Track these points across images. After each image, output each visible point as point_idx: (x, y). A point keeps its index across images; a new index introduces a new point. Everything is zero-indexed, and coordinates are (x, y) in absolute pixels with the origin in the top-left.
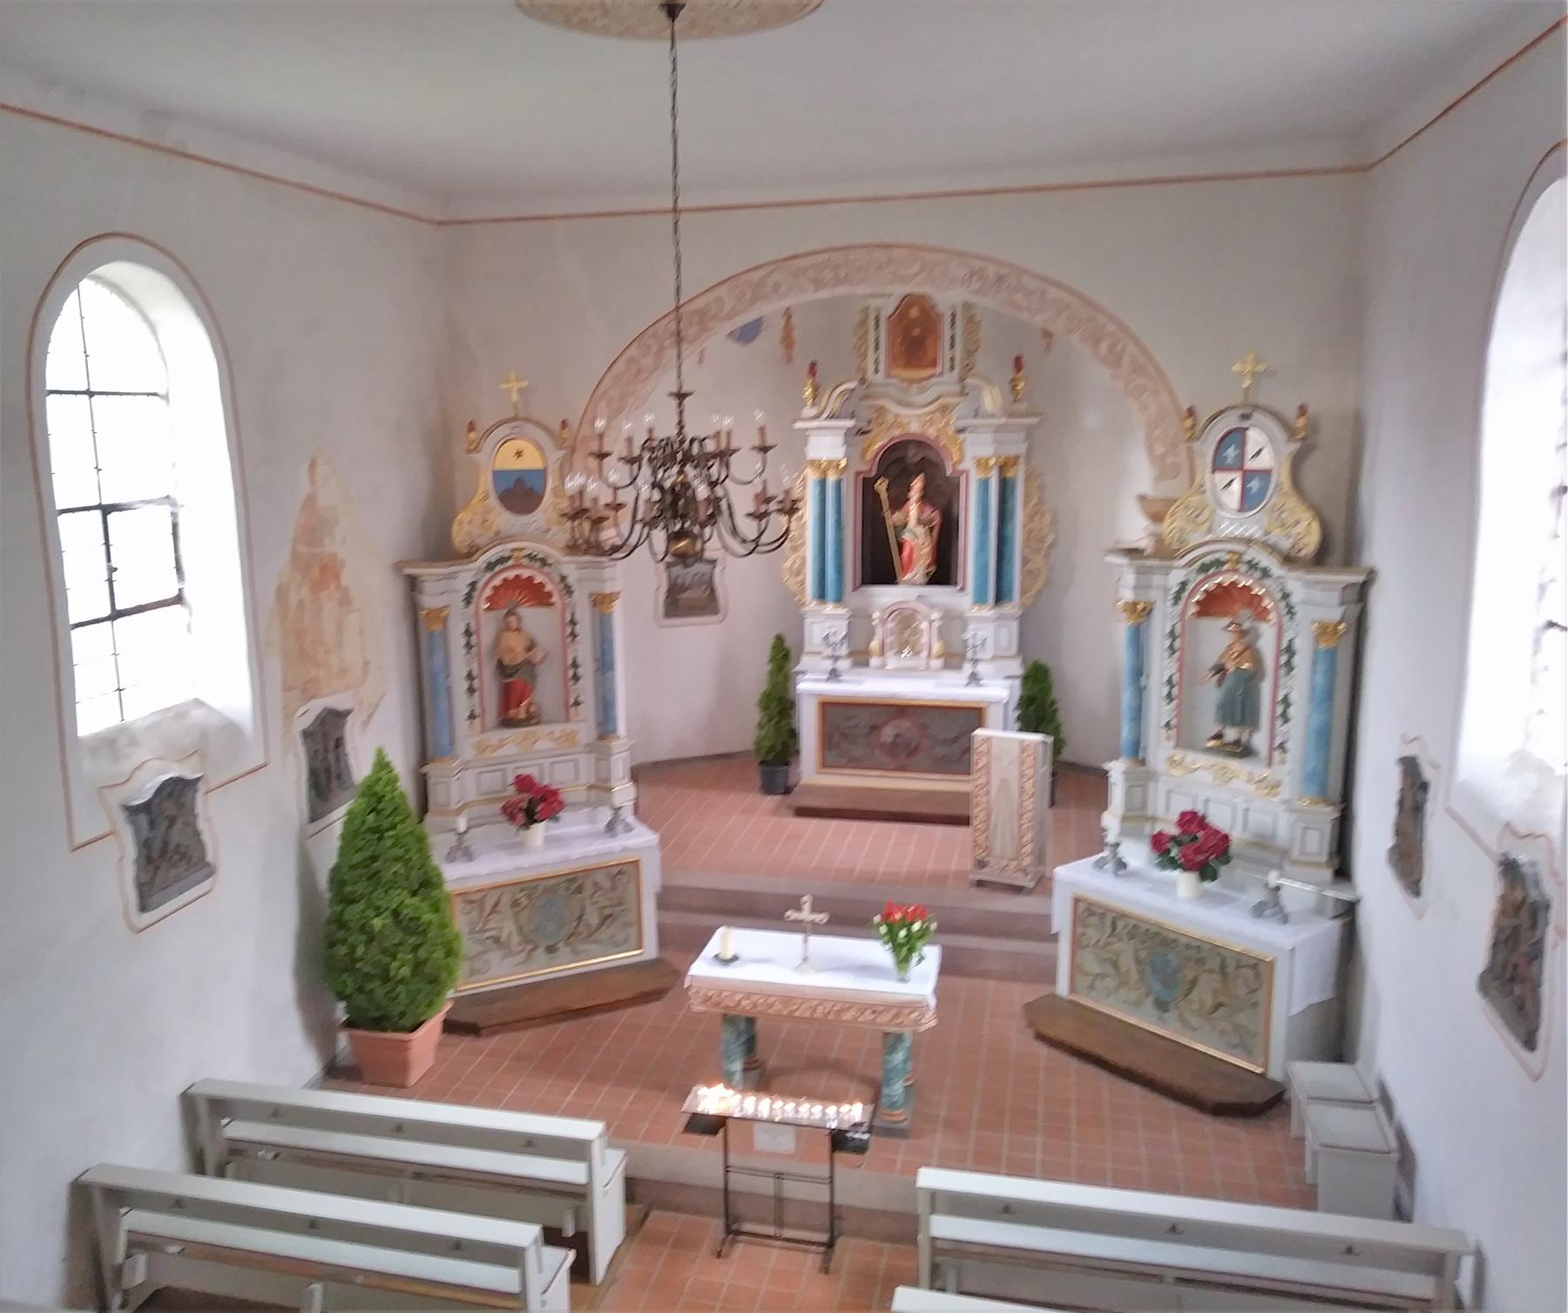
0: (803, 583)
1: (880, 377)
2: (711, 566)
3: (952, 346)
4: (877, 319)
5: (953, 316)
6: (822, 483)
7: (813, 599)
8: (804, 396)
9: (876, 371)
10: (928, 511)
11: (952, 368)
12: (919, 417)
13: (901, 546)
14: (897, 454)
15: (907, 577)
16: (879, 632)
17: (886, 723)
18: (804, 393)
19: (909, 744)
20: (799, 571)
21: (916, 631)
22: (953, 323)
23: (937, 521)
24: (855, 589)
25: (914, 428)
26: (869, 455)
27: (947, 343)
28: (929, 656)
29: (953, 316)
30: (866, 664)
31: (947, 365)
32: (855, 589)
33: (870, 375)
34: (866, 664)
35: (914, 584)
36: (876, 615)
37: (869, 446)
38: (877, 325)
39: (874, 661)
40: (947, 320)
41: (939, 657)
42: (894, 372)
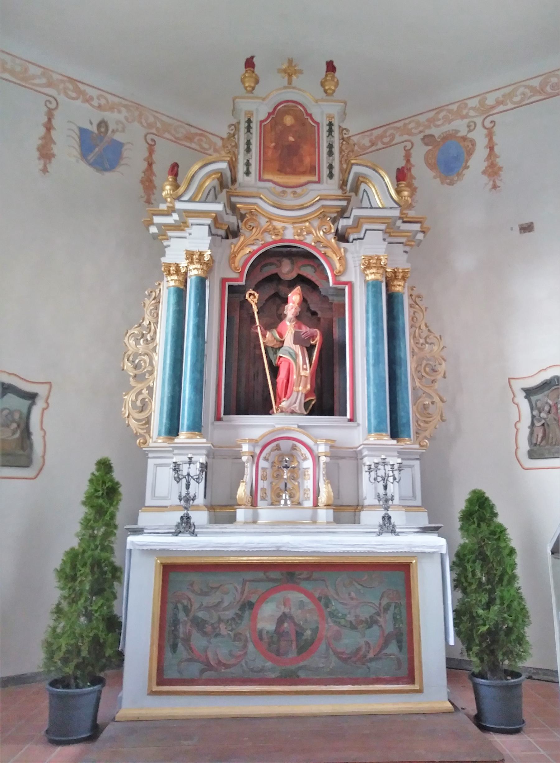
0: (148, 421)
1: (253, 178)
2: (29, 402)
3: (330, 153)
4: (249, 121)
5: (330, 124)
6: (181, 294)
7: (159, 435)
8: (164, 194)
9: (248, 173)
10: (305, 329)
11: (331, 176)
12: (295, 221)
13: (275, 370)
14: (269, 271)
15: (284, 404)
16: (249, 472)
17: (263, 599)
18: (163, 189)
19: (299, 634)
20: (144, 407)
21: (296, 474)
22: (330, 131)
23: (317, 341)
24: (218, 418)
25: (290, 234)
26: (240, 260)
27: (325, 150)
28: (316, 504)
29: (330, 124)
30: (232, 519)
31: (325, 172)
32: (218, 418)
33: (241, 175)
34: (232, 519)
35: (293, 413)
36: (245, 448)
37: (241, 248)
38: (249, 128)
39: (241, 514)
40: (325, 129)
41: (328, 506)
42: (267, 176)
